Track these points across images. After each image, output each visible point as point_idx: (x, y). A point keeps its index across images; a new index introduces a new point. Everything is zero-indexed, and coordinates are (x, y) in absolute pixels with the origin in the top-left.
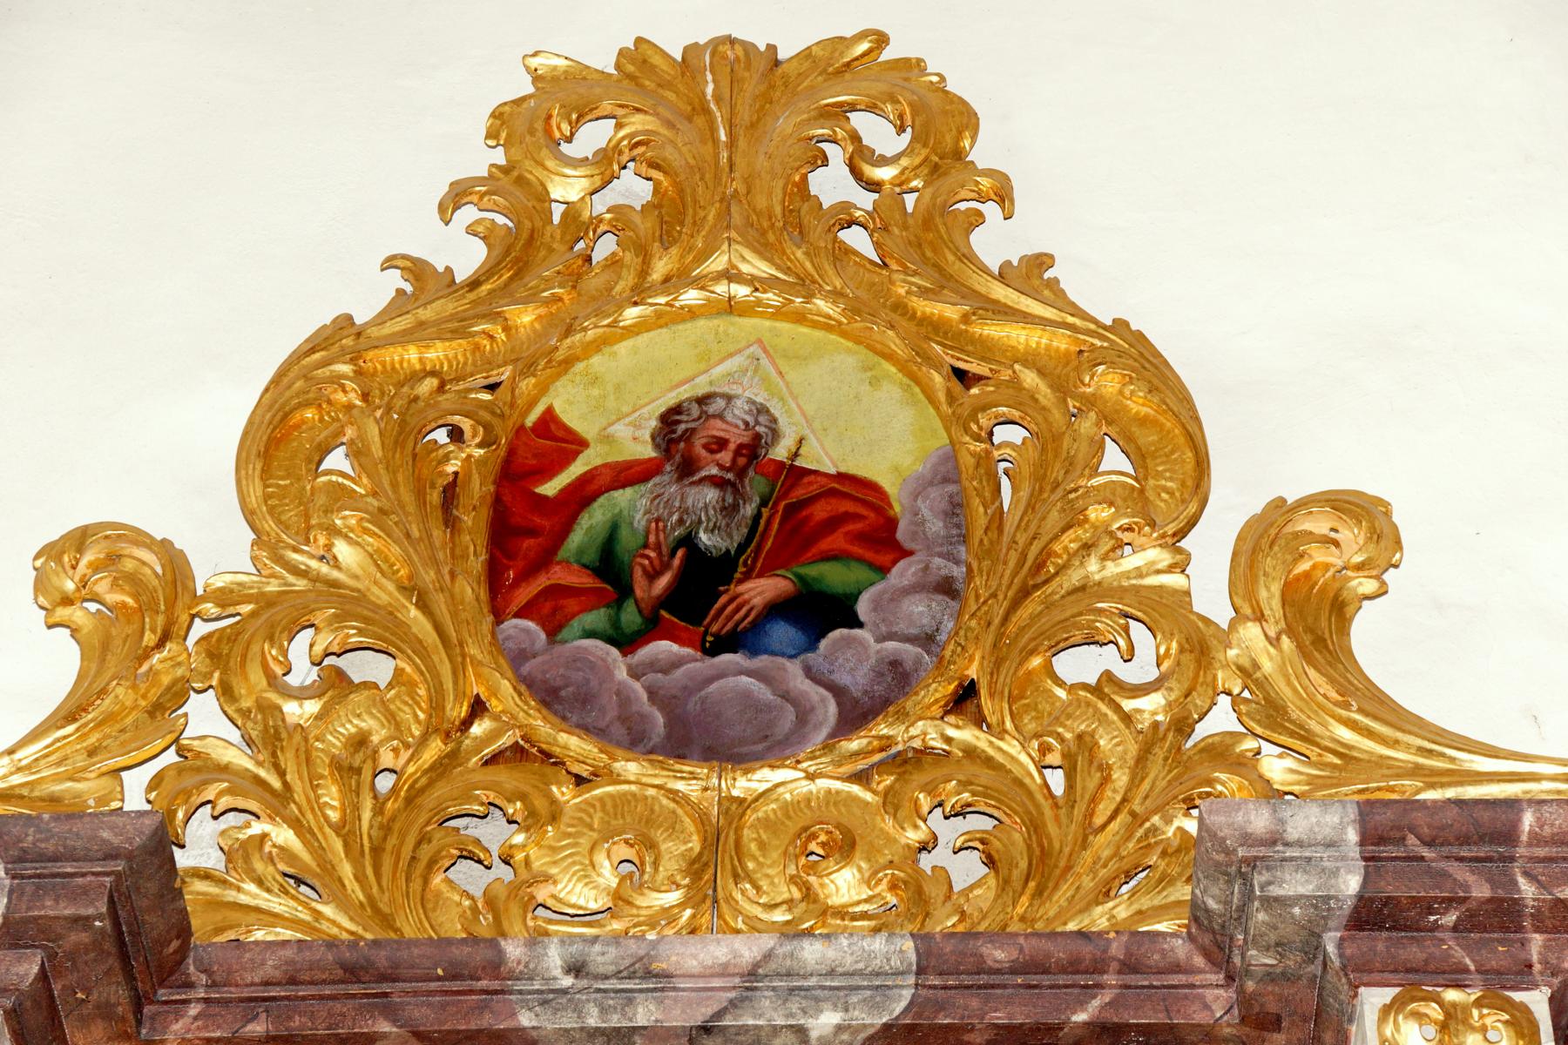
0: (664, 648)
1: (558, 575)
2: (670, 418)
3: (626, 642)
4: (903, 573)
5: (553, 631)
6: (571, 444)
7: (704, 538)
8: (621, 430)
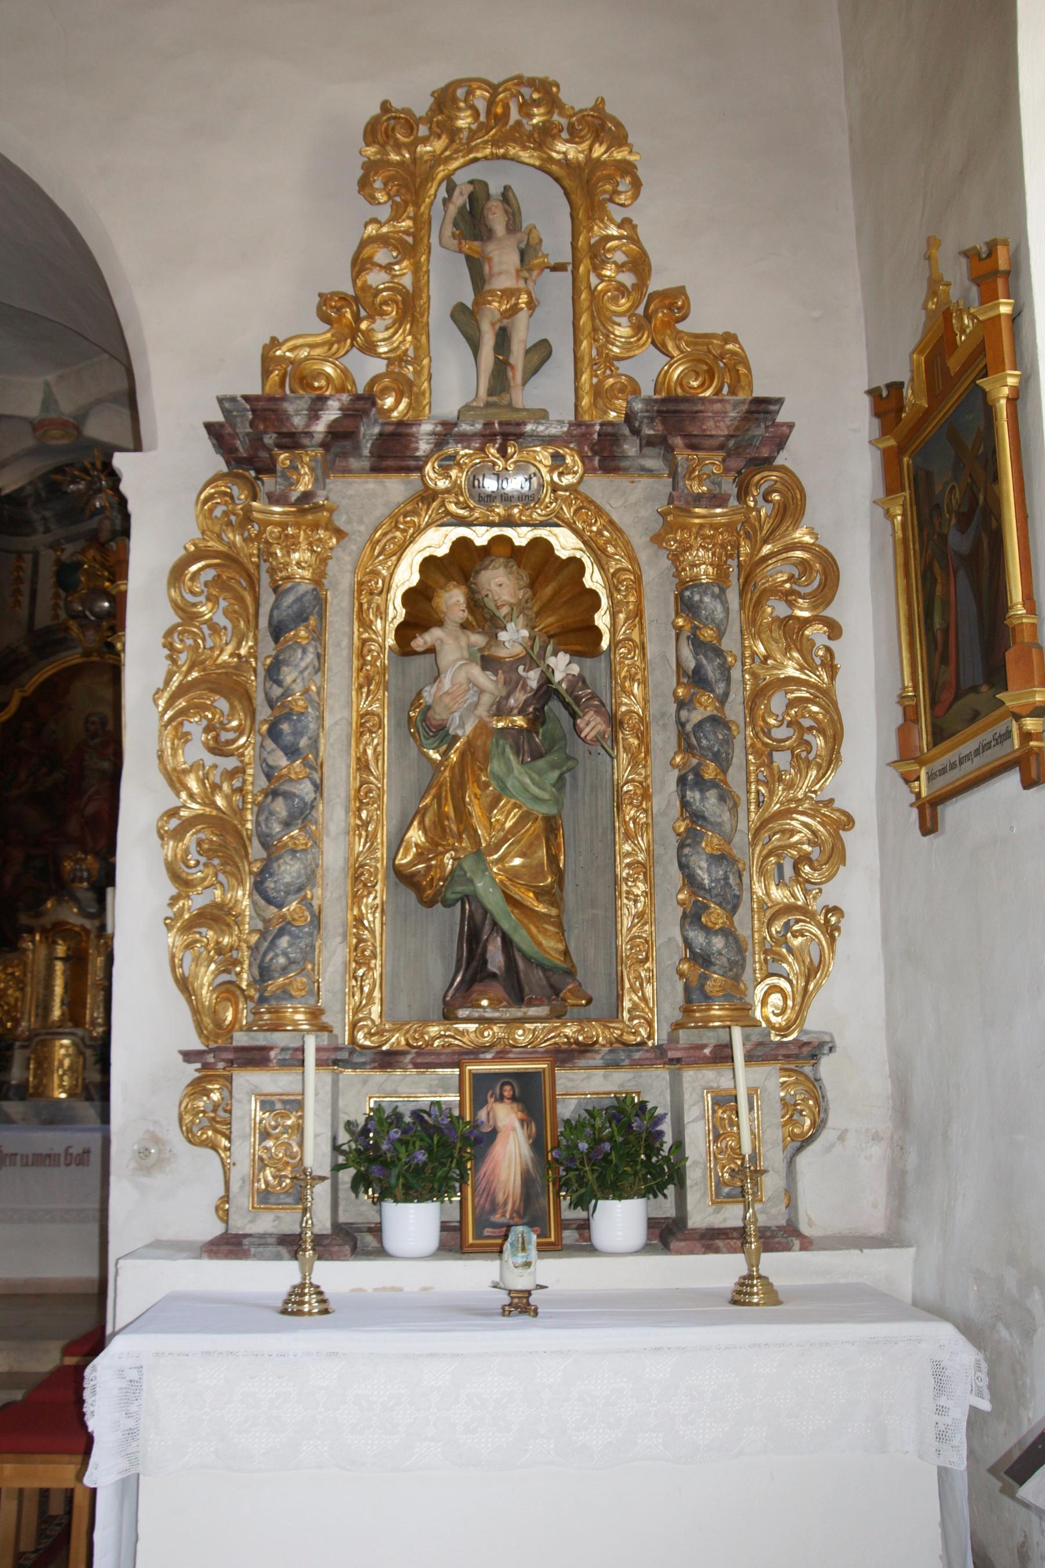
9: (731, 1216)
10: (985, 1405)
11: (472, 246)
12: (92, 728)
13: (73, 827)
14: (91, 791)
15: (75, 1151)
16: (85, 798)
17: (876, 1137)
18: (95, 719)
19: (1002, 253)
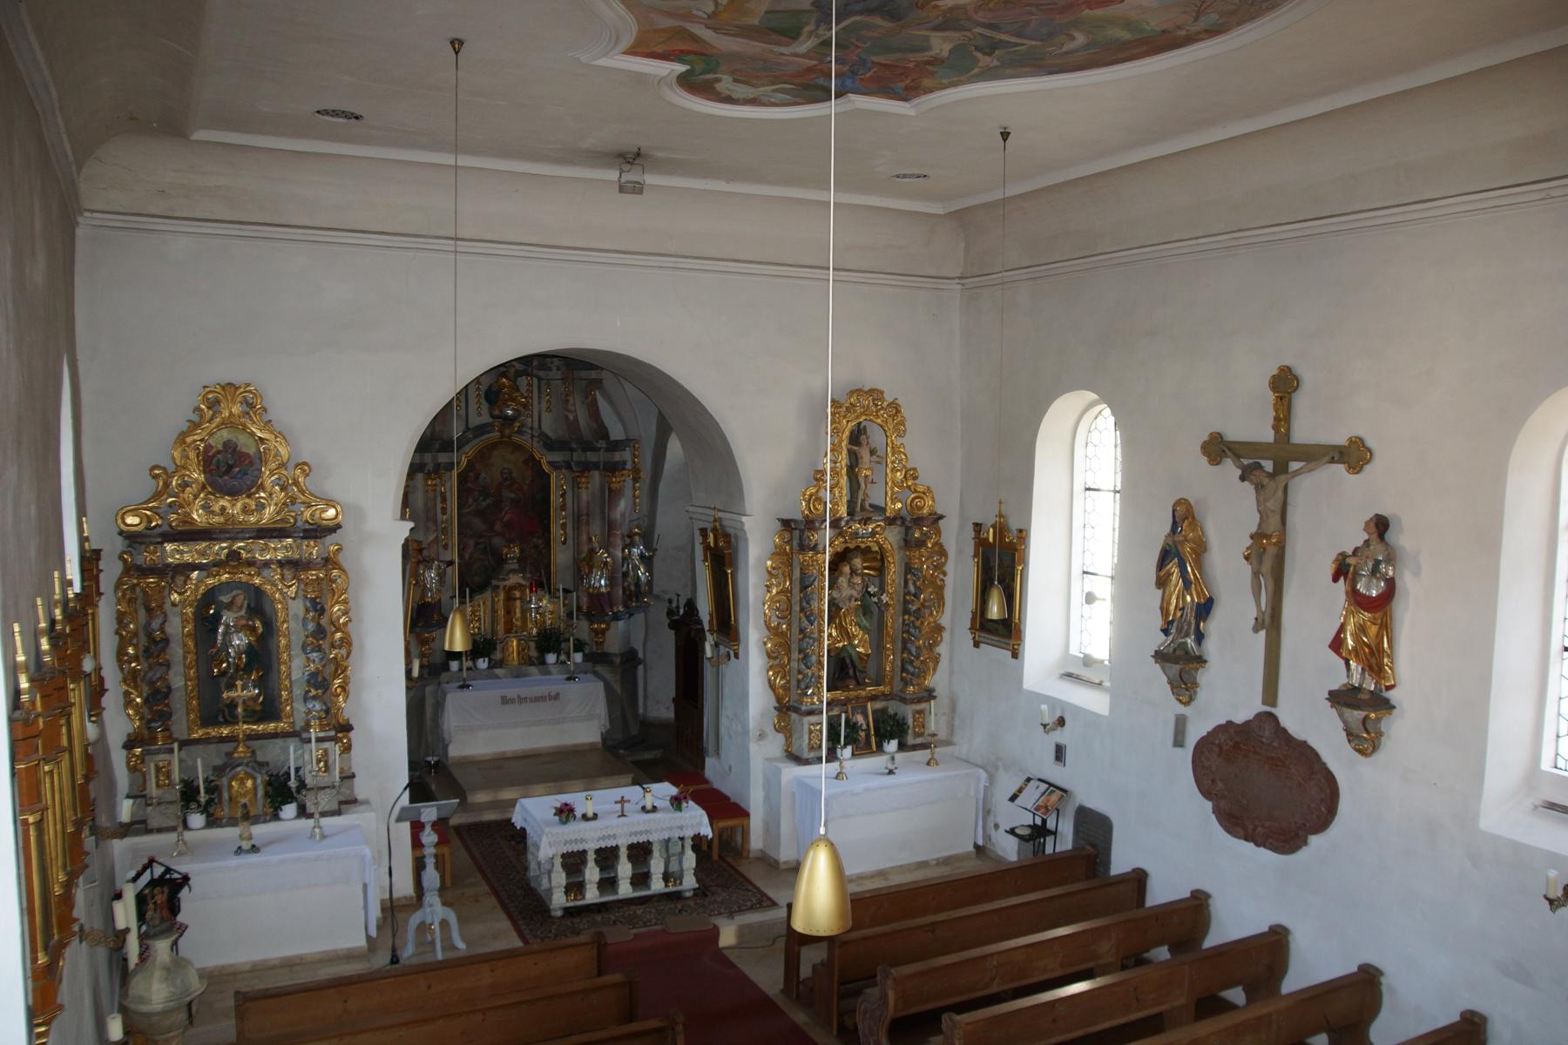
0: (226, 478)
1: (212, 467)
2: (224, 443)
3: (221, 477)
4: (254, 468)
5: (212, 475)
6: (212, 447)
7: (230, 462)
8: (219, 446)
9: (919, 741)
10: (987, 784)
11: (855, 448)
12: (505, 476)
13: (498, 527)
14: (507, 508)
15: (553, 694)
16: (503, 513)
17: (944, 714)
18: (506, 471)
19: (1024, 533)
